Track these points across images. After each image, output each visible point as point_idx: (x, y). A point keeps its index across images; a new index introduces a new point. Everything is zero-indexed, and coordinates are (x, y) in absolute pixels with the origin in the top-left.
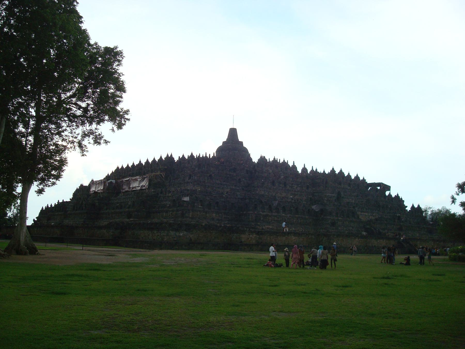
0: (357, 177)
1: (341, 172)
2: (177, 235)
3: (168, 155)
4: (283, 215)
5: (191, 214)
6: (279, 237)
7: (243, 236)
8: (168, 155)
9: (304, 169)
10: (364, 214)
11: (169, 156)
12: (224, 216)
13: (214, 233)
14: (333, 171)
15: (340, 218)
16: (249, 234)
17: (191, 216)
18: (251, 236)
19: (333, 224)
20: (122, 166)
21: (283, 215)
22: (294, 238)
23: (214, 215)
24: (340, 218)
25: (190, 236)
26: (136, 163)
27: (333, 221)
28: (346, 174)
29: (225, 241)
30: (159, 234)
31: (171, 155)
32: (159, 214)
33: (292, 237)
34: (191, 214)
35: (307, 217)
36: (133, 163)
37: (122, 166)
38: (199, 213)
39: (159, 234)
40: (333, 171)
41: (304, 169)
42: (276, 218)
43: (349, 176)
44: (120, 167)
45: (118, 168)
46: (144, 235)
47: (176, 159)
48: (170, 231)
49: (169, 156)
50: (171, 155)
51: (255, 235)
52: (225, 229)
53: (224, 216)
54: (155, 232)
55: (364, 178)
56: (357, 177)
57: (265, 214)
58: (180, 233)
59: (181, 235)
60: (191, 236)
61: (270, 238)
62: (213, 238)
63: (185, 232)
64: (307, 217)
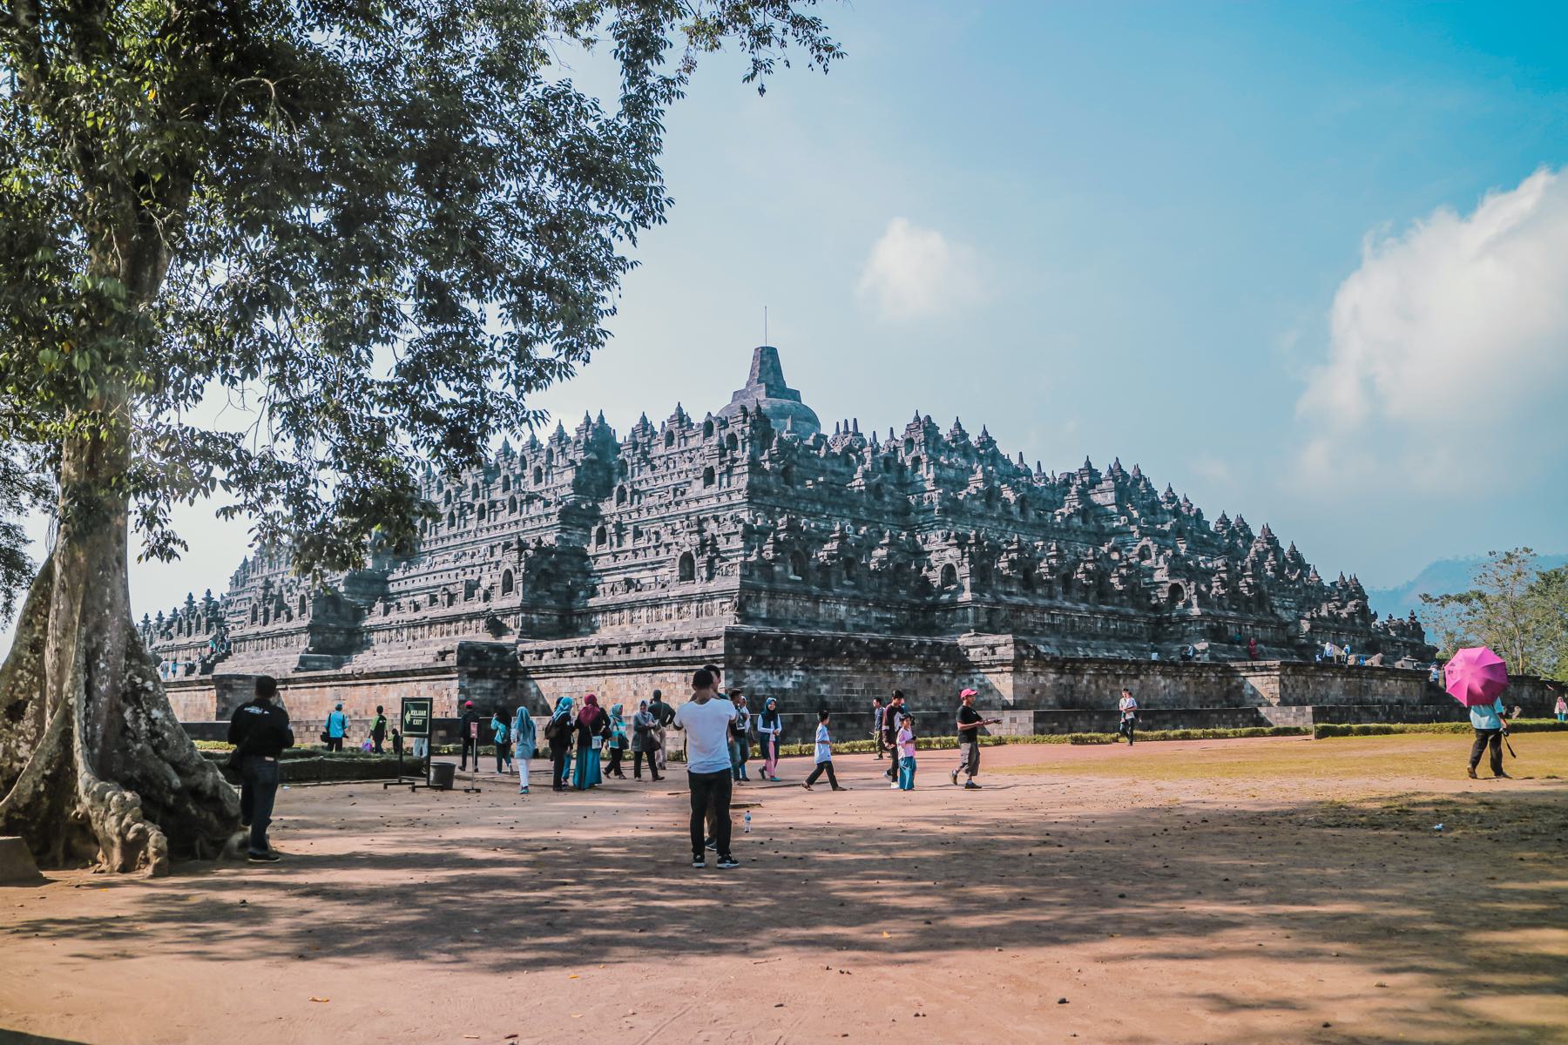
2: (774, 686)
3: (588, 418)
4: (1067, 604)
5: (764, 605)
8: (588, 418)
11: (594, 420)
12: (874, 614)
13: (901, 675)
16: (1036, 674)
17: (764, 616)
18: (1041, 679)
21: (1067, 604)
22: (1162, 684)
23: (843, 608)
24: (1231, 614)
25: (819, 690)
29: (940, 704)
31: (601, 418)
33: (1159, 678)
34: (764, 605)
35: (1132, 612)
38: (790, 602)
42: (1047, 619)
46: (608, 693)
48: (747, 672)
49: (594, 420)
50: (601, 418)
51: (1052, 676)
52: (938, 658)
57: (1016, 600)
58: (782, 678)
59: (788, 685)
61: (1097, 686)
63: (801, 673)
64: (1132, 612)
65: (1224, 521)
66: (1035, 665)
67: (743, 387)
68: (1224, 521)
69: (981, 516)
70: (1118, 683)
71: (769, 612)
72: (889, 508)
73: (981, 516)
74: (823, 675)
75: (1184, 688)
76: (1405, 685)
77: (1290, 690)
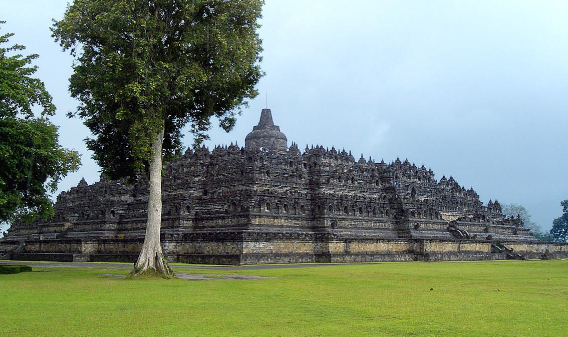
5: (257, 219)
6: (367, 245)
7: (330, 245)
9: (362, 159)
10: (444, 213)
15: (422, 220)
19: (416, 227)
22: (383, 245)
27: (416, 224)
30: (235, 246)
32: (211, 221)
39: (235, 246)
41: (362, 159)
53: (293, 222)
54: (229, 244)
55: (430, 170)
59: (261, 246)
60: (272, 247)
62: (295, 248)
65: (444, 178)
66: (337, 240)
67: (257, 125)
68: (444, 178)
69: (337, 186)
70: (366, 246)
71: (259, 222)
72: (304, 182)
73: (337, 186)
74: (272, 243)
75: (392, 247)
76: (480, 245)
77: (428, 248)
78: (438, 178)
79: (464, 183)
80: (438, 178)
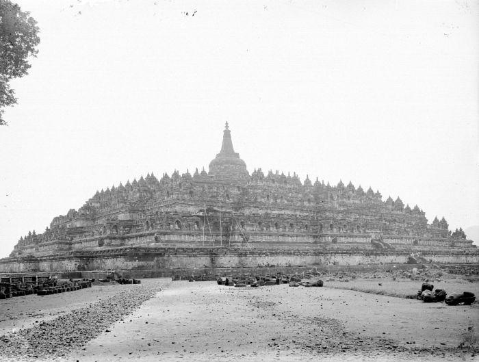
0: (370, 191)
1: (350, 186)
3: (148, 175)
8: (148, 175)
14: (341, 184)
20: (102, 191)
26: (117, 186)
28: (356, 188)
31: (152, 174)
36: (113, 187)
37: (102, 191)
40: (341, 184)
41: (308, 181)
43: (360, 189)
44: (100, 192)
45: (98, 192)
47: (159, 178)
56: (370, 191)
65: (390, 199)
68: (390, 199)
78: (384, 199)
79: (409, 202)
80: (384, 199)
